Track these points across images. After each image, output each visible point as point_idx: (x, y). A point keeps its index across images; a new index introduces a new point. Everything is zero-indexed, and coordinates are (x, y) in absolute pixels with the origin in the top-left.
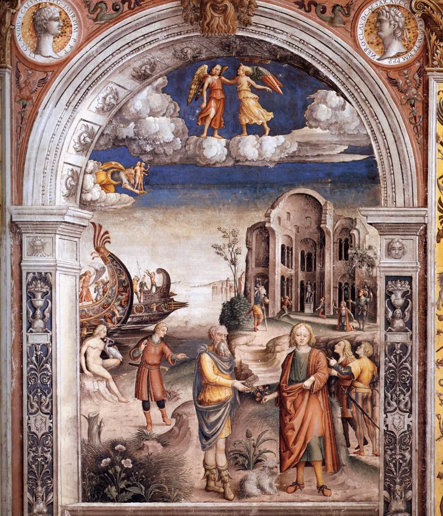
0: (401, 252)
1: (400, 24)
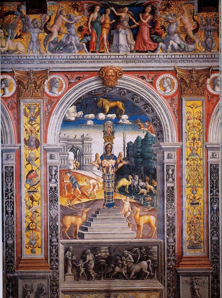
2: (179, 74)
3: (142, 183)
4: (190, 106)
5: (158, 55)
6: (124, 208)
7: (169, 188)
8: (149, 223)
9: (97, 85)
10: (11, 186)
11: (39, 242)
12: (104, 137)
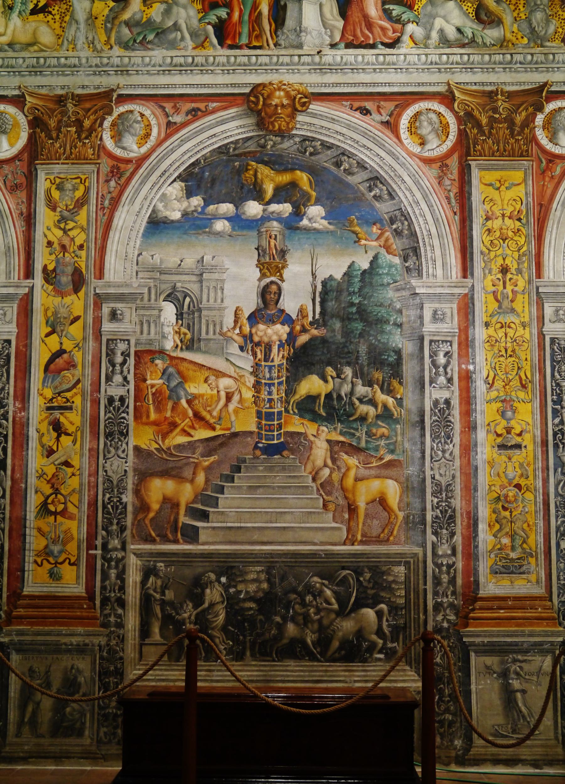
2: (462, 102)
3: (361, 390)
4: (490, 185)
5: (405, 55)
6: (311, 458)
7: (436, 403)
8: (382, 501)
9: (243, 130)
11: (72, 547)
12: (260, 265)
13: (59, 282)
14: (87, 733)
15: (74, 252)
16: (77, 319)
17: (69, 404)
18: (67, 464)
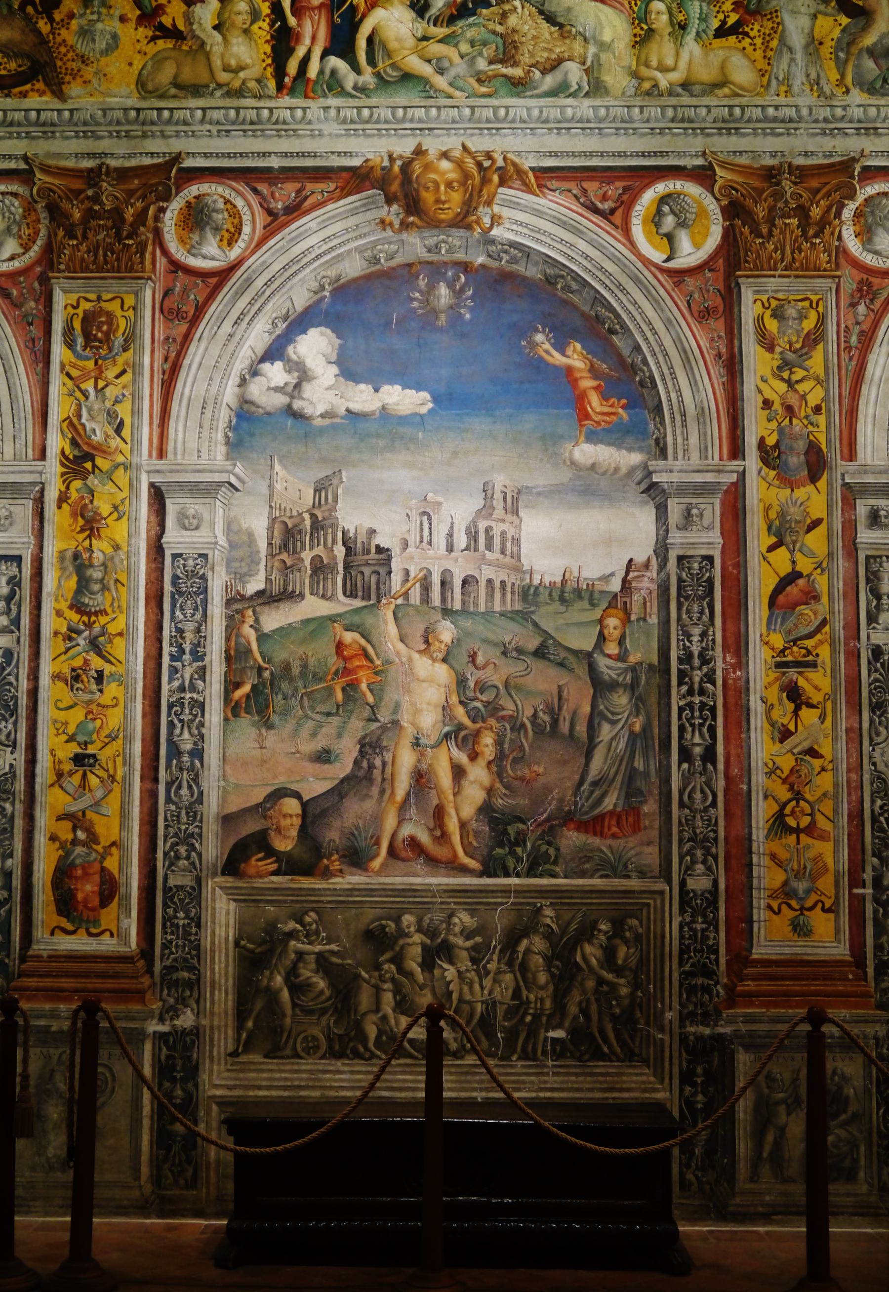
0: (7, 522)
1: (17, 217)
10: (701, 641)
11: (826, 884)
13: (786, 463)
14: (862, 1175)
15: (807, 417)
16: (817, 523)
17: (811, 658)
18: (813, 752)
